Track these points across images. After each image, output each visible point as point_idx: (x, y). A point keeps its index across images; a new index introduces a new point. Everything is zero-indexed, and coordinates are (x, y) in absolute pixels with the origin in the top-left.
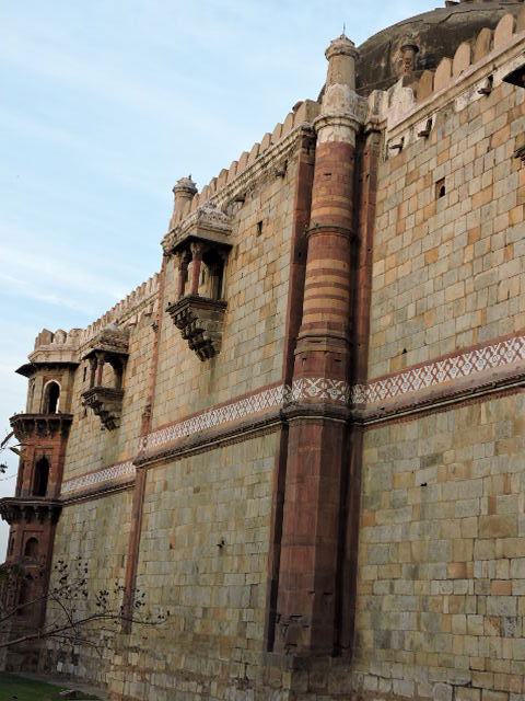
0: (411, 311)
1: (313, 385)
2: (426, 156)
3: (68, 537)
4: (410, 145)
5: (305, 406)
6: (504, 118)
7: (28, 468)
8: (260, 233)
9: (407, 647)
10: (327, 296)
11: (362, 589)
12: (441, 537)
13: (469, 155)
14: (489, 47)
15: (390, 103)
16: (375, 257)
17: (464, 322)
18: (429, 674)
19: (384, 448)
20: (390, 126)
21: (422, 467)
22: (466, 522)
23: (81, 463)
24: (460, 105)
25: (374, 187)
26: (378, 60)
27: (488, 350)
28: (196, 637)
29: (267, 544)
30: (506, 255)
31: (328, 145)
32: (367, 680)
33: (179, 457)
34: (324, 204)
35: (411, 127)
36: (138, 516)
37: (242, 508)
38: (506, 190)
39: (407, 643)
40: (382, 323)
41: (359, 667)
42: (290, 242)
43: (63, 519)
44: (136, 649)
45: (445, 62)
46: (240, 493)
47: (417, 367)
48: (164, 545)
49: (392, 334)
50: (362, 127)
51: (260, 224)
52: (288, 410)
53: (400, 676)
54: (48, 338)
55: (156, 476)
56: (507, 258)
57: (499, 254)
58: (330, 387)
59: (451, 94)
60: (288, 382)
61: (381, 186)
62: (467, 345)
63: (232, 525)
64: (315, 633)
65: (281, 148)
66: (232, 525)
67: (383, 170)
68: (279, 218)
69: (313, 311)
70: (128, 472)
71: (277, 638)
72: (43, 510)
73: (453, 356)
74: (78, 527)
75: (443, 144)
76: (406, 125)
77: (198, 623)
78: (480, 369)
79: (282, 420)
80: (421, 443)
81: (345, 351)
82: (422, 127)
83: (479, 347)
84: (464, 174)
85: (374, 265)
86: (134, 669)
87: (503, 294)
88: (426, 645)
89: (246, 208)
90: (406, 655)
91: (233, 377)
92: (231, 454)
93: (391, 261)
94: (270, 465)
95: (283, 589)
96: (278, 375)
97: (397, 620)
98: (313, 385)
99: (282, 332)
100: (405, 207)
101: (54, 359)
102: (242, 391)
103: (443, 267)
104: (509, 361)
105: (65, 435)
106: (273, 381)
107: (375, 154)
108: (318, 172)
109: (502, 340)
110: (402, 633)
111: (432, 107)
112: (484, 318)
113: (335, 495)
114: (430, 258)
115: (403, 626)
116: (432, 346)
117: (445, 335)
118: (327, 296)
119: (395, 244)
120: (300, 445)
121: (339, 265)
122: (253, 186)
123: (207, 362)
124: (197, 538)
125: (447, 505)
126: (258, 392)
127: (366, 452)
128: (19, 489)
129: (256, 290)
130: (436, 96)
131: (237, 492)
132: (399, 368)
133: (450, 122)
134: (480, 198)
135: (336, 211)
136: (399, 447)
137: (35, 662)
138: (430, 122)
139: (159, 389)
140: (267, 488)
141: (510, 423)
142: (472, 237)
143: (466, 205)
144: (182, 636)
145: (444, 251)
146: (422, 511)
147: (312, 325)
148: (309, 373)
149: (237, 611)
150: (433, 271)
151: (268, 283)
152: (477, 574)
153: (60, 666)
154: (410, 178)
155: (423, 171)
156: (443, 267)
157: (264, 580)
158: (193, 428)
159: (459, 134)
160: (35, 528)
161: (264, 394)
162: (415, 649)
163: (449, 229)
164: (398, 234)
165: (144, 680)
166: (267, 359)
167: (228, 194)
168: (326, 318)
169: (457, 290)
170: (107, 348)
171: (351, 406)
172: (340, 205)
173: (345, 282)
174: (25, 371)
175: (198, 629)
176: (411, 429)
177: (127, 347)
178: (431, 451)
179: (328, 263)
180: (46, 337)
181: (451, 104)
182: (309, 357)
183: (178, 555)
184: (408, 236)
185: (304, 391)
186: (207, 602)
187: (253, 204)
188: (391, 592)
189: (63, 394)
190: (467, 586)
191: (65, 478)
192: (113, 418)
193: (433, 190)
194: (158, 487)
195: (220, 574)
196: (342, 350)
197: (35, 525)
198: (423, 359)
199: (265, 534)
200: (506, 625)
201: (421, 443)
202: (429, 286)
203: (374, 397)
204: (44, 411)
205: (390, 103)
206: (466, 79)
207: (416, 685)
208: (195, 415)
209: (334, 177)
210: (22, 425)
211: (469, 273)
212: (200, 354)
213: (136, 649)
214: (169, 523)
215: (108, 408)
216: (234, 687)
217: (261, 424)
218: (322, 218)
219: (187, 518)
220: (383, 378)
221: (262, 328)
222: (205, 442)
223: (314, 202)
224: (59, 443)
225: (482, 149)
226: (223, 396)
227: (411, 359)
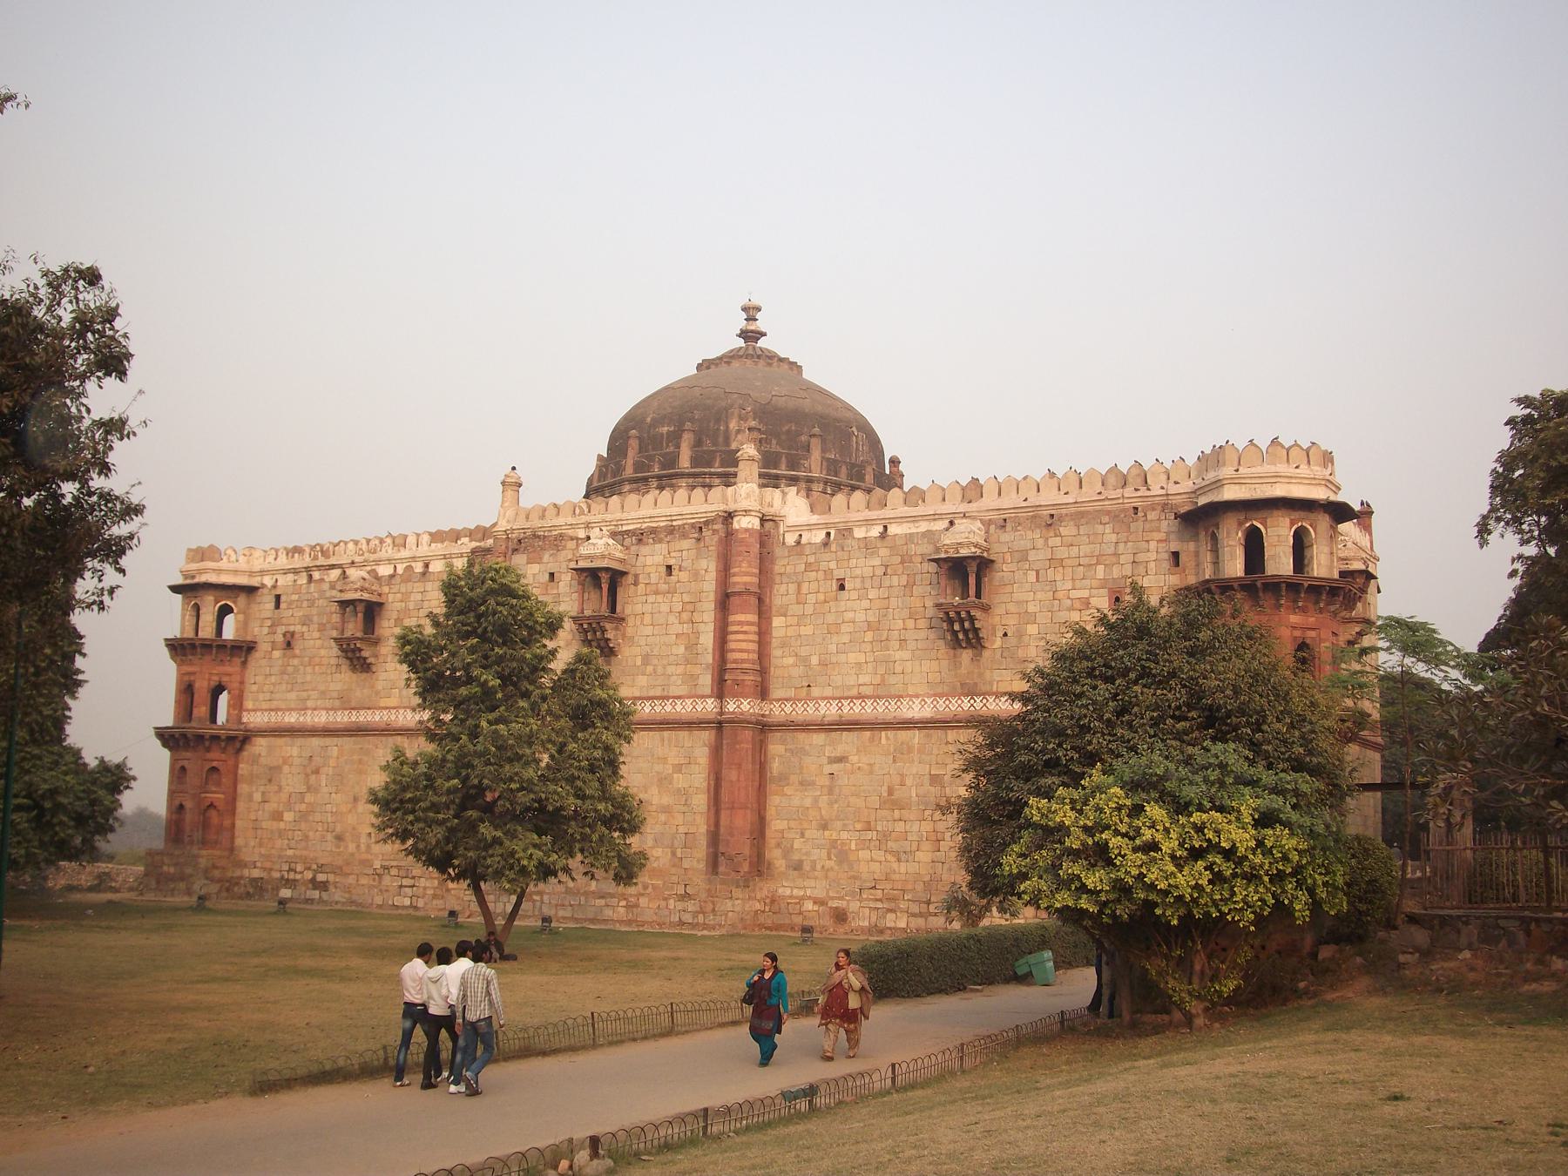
0: (815, 660)
13: (868, 572)
24: (859, 533)
31: (747, 530)
40: (782, 661)
56: (901, 648)
63: (654, 790)
79: (719, 725)
82: (819, 536)
83: (879, 697)
87: (898, 669)
102: (658, 693)
103: (846, 639)
105: (244, 663)
112: (883, 680)
114: (834, 629)
121: (753, 618)
138: (828, 534)
143: (866, 604)
145: (844, 628)
146: (830, 792)
150: (835, 638)
154: (808, 567)
155: (823, 566)
163: (849, 615)
169: (853, 657)
174: (175, 589)
176: (819, 738)
181: (850, 530)
190: (869, 835)
191: (249, 704)
193: (835, 587)
199: (701, 801)
202: (833, 648)
210: (178, 648)
221: (681, 650)
225: (880, 572)
227: (815, 692)
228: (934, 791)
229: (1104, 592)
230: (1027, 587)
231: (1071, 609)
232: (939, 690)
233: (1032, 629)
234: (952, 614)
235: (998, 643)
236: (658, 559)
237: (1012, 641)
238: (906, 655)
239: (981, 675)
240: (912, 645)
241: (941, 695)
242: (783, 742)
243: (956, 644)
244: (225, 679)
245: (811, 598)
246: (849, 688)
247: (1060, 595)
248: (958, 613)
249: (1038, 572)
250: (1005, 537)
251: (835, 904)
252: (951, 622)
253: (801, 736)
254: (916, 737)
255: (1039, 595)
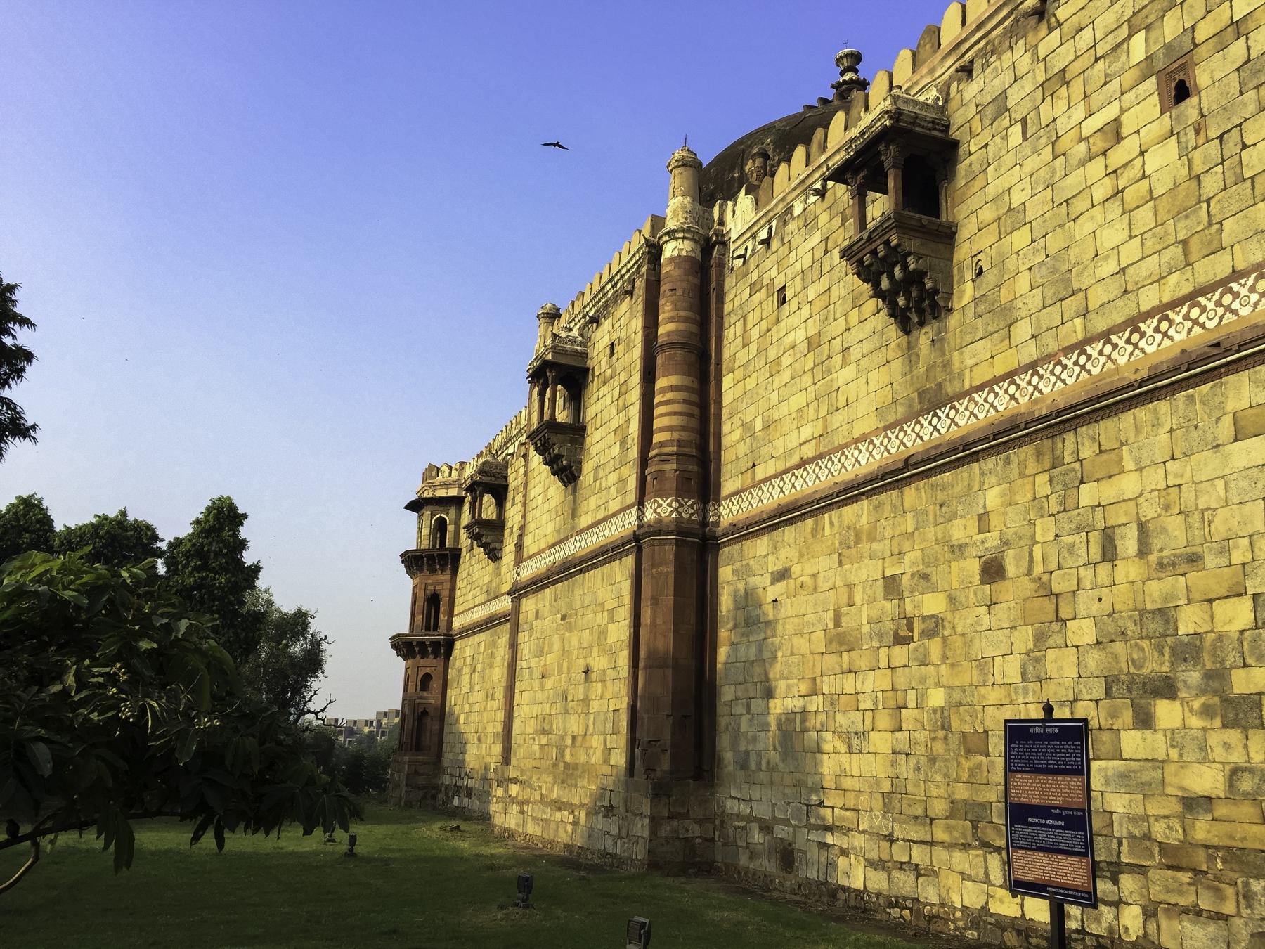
1: (665, 505)
2: (768, 264)
3: (460, 670)
4: (753, 253)
5: (658, 527)
6: (839, 219)
7: (420, 603)
8: (612, 354)
9: (764, 768)
10: (675, 414)
11: (721, 710)
12: (792, 654)
13: (807, 261)
14: (824, 147)
15: (734, 212)
16: (724, 372)
17: (807, 432)
18: (784, 794)
19: (737, 565)
20: (734, 236)
21: (773, 583)
22: (814, 636)
23: (470, 596)
24: (798, 210)
25: (721, 300)
26: (732, 170)
27: (830, 459)
28: (567, 766)
29: (626, 668)
30: (844, 359)
31: (672, 259)
32: (729, 803)
33: (547, 586)
34: (671, 320)
35: (754, 236)
36: (514, 646)
37: (603, 633)
38: (843, 293)
39: (764, 763)
41: (720, 790)
42: (638, 361)
43: (456, 653)
44: (514, 781)
45: (783, 166)
46: (602, 618)
47: (765, 480)
48: (537, 674)
49: (742, 449)
50: (708, 239)
51: (612, 345)
52: (641, 531)
53: (758, 797)
54: (434, 473)
55: (529, 605)
56: (845, 363)
57: (838, 359)
58: (681, 505)
59: (789, 198)
60: (641, 503)
61: (728, 299)
62: (810, 455)
64: (674, 758)
65: (629, 266)
66: (595, 650)
67: (729, 282)
68: (629, 337)
69: (662, 430)
70: (504, 604)
71: (637, 764)
72: (436, 645)
73: (798, 467)
74: (469, 660)
75: (783, 251)
76: (748, 235)
77: (568, 751)
78: (823, 479)
79: (637, 542)
80: (771, 558)
81: (696, 468)
82: (763, 235)
83: (821, 456)
84: (803, 280)
85: (724, 379)
86: (513, 800)
87: (842, 403)
88: (781, 765)
89: (600, 329)
90: (763, 776)
91: (594, 501)
92: (594, 578)
93: (739, 373)
94: (627, 587)
95: (643, 716)
96: (632, 498)
97: (754, 740)
98: (665, 505)
99: (634, 452)
100: (750, 317)
101: (441, 493)
102: (600, 515)
104: (849, 468)
105: (455, 571)
106: (628, 503)
107: (721, 265)
108: (664, 288)
109: (842, 448)
110: (759, 754)
111: (771, 214)
113: (691, 617)
114: (775, 368)
115: (760, 747)
116: (778, 458)
117: (791, 446)
118: (675, 414)
119: (742, 357)
120: (653, 566)
122: (606, 306)
123: (570, 487)
124: (565, 665)
125: (796, 620)
126: (614, 515)
127: (721, 571)
128: (412, 624)
129: (611, 414)
130: (774, 202)
131: (599, 617)
132: (749, 482)
133: (788, 228)
134: (819, 304)
135: (682, 326)
136: (751, 563)
137: (434, 797)
138: (771, 229)
139: (529, 517)
140: (624, 613)
141: (852, 533)
142: (813, 344)
143: (806, 311)
144: (555, 765)
145: (786, 360)
147: (662, 444)
148: (661, 494)
149: (602, 737)
151: (621, 402)
152: (826, 691)
153: (456, 801)
154: (754, 288)
156: (786, 376)
157: (625, 705)
158: (560, 555)
159: (798, 240)
160: (429, 664)
161: (620, 516)
162: (772, 769)
163: (789, 339)
164: (744, 346)
165: (522, 812)
166: (622, 481)
167: (584, 317)
168: (676, 435)
169: (798, 401)
170: (486, 479)
171: (704, 523)
172: (686, 320)
173: (695, 398)
175: (568, 758)
176: (761, 545)
177: (506, 478)
178: (780, 566)
179: (673, 380)
180: (432, 471)
182: (659, 476)
183: (549, 683)
184: (753, 348)
185: (655, 511)
186: (575, 729)
187: (606, 324)
188: (748, 712)
189: (450, 528)
191: (456, 612)
192: (495, 549)
194: (531, 616)
195: (586, 701)
196: (693, 468)
197: (430, 660)
198: (771, 472)
200: (855, 741)
201: (771, 558)
202: (774, 397)
203: (729, 513)
204: (434, 546)
205: (734, 212)
206: (803, 181)
207: (774, 805)
208: (561, 542)
209: (679, 292)
210: (413, 561)
211: (810, 381)
212: (561, 480)
213: (514, 781)
214: (540, 653)
215: (489, 540)
216: (600, 816)
217: (617, 547)
218: (669, 334)
219: (557, 645)
220: (734, 494)
221: (616, 450)
222: (568, 569)
223: (660, 318)
224: (449, 577)
225: (819, 253)
226: (585, 521)
227: (761, 473)
228: (889, 607)
229: (1151, 83)
230: (1009, 159)
231: (1083, 163)
232: (891, 419)
233: (1021, 238)
234: (867, 260)
235: (965, 292)
236: (606, 341)
237: (990, 278)
238: (849, 372)
239: (947, 365)
240: (856, 353)
241: (890, 427)
242: (731, 561)
243: (905, 321)
244: (439, 587)
245: (755, 333)
246: (790, 453)
247: (1063, 145)
248: (874, 253)
249: (1024, 121)
250: (971, 89)
251: (781, 832)
252: (867, 273)
253: (748, 544)
254: (859, 513)
255: (1030, 165)
